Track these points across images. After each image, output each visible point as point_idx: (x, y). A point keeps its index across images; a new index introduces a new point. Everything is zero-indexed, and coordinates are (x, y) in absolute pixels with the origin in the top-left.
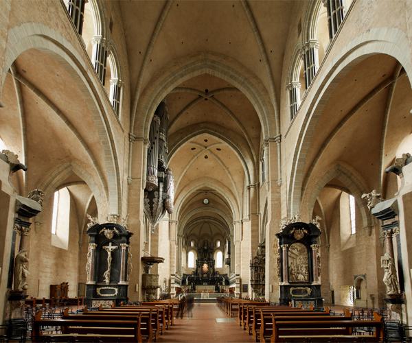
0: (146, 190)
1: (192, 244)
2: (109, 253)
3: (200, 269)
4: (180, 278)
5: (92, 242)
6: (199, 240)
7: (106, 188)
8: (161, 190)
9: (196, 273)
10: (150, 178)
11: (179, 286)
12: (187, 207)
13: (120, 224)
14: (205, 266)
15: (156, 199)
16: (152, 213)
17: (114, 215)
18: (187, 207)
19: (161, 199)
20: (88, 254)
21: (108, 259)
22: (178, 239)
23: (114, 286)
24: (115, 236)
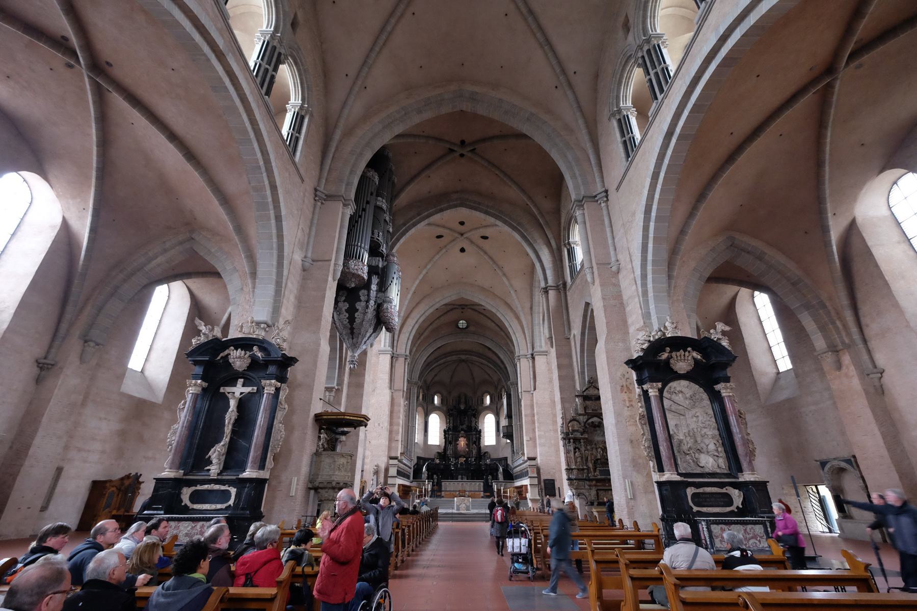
0: (341, 287)
1: (436, 400)
2: (233, 403)
3: (450, 447)
4: (409, 464)
5: (195, 377)
6: (450, 393)
7: (254, 274)
8: (374, 287)
9: (443, 455)
10: (352, 263)
11: (407, 483)
12: (426, 334)
13: (269, 339)
14: (462, 442)
15: (363, 304)
16: (352, 329)
17: (258, 323)
18: (426, 334)
19: (372, 303)
20: (181, 405)
21: (227, 416)
22: (409, 389)
23: (230, 483)
24: (255, 365)
